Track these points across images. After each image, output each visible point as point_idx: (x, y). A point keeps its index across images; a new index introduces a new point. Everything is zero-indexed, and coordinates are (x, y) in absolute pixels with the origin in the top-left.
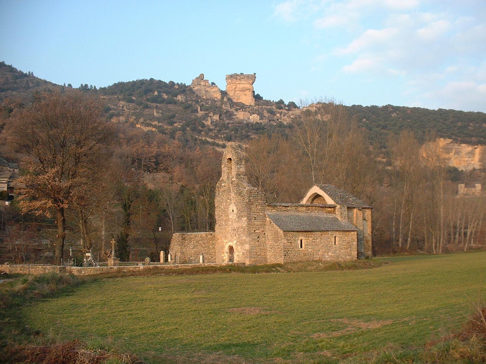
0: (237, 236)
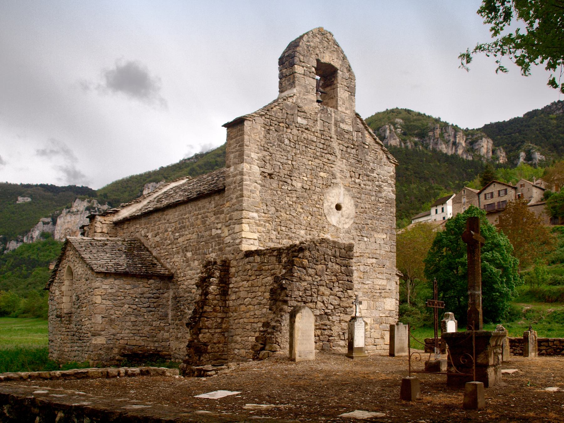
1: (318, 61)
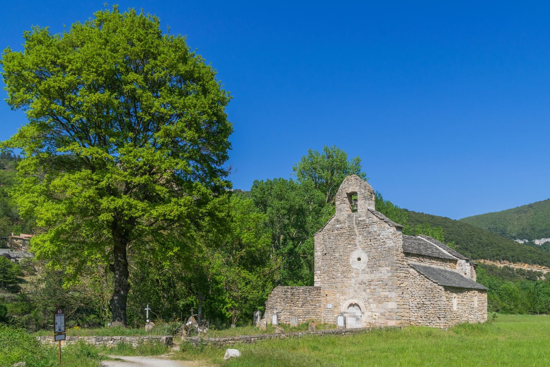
0: (368, 291)
1: (347, 193)
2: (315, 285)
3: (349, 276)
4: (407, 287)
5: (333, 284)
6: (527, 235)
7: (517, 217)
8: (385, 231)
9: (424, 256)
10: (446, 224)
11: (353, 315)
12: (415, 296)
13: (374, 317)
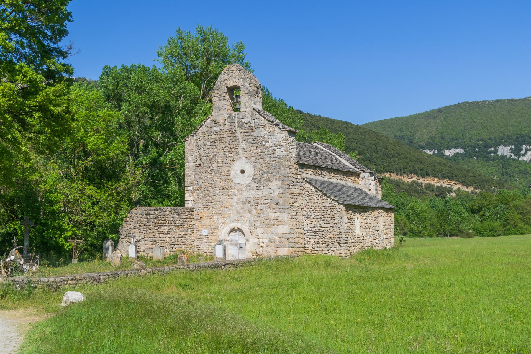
0: (254, 211)
1: (227, 87)
2: (187, 205)
3: (229, 193)
4: (301, 207)
5: (210, 204)
6: (437, 144)
7: (425, 123)
8: (275, 137)
9: (321, 168)
10: (346, 130)
11: (235, 242)
12: (312, 217)
13: (262, 244)
